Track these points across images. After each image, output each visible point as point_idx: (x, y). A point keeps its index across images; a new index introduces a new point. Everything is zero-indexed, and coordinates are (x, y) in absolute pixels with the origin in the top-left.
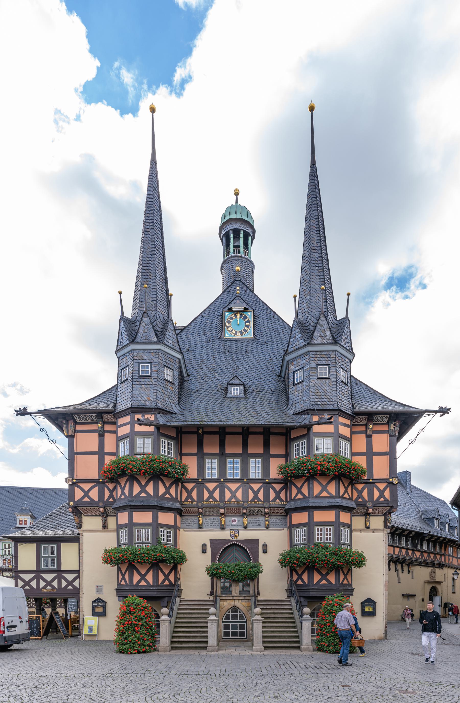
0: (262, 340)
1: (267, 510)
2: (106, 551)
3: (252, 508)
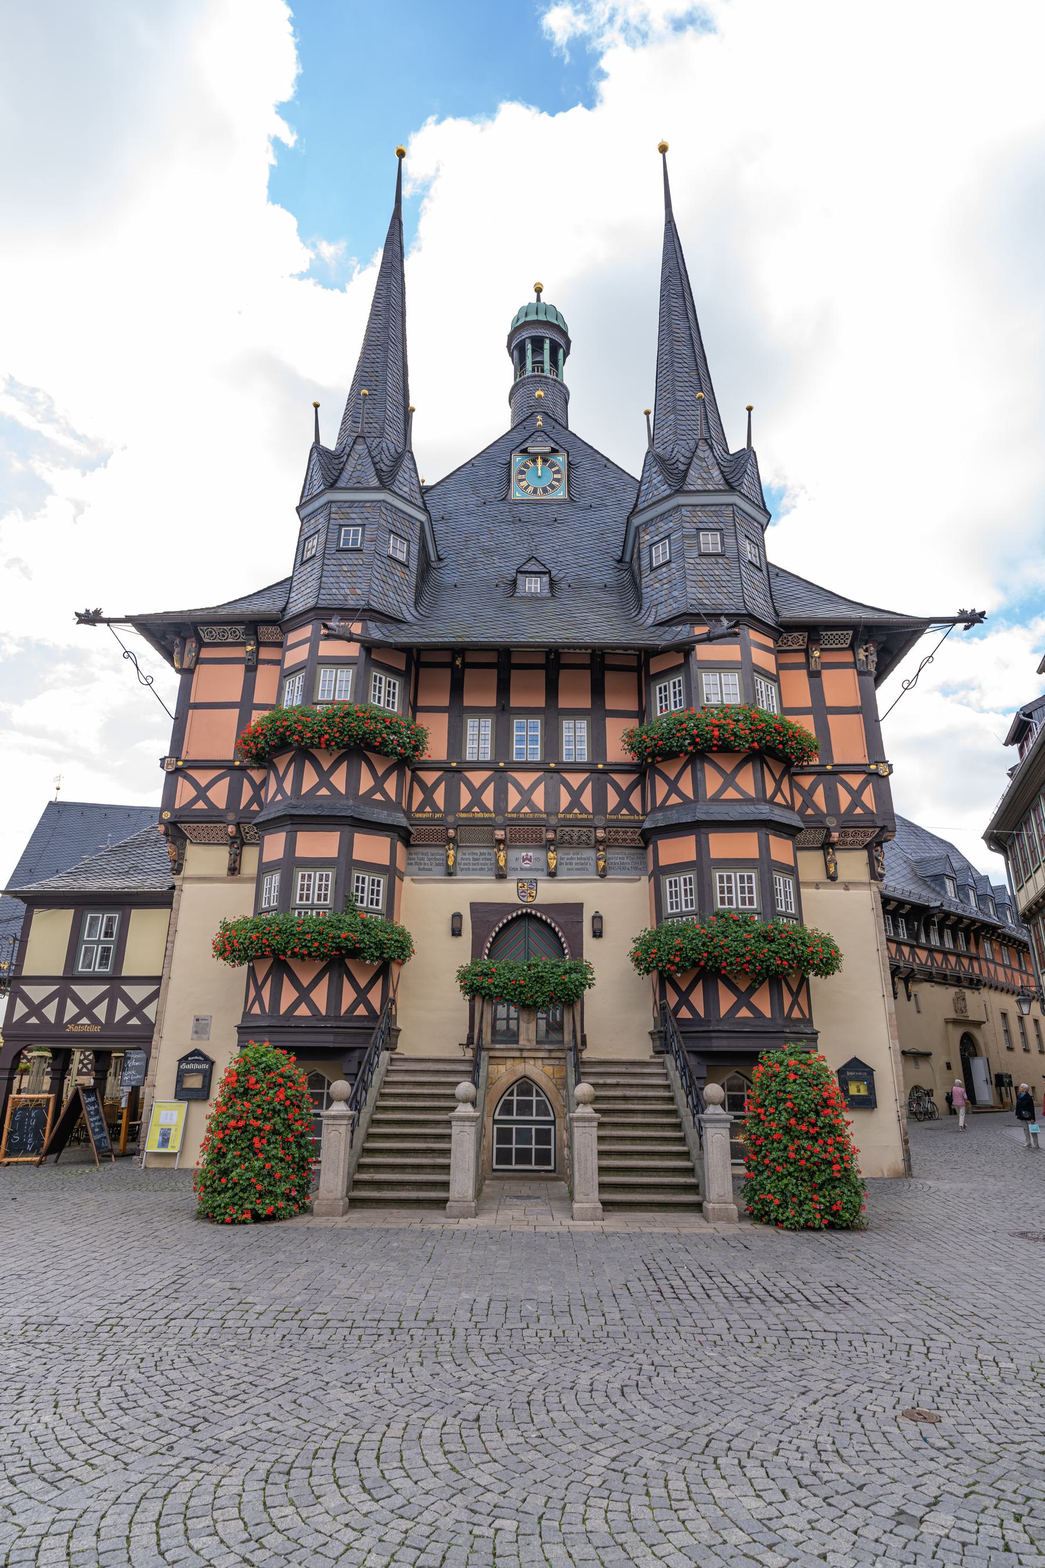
0: (583, 502)
1: (600, 834)
2: (225, 927)
3: (567, 829)
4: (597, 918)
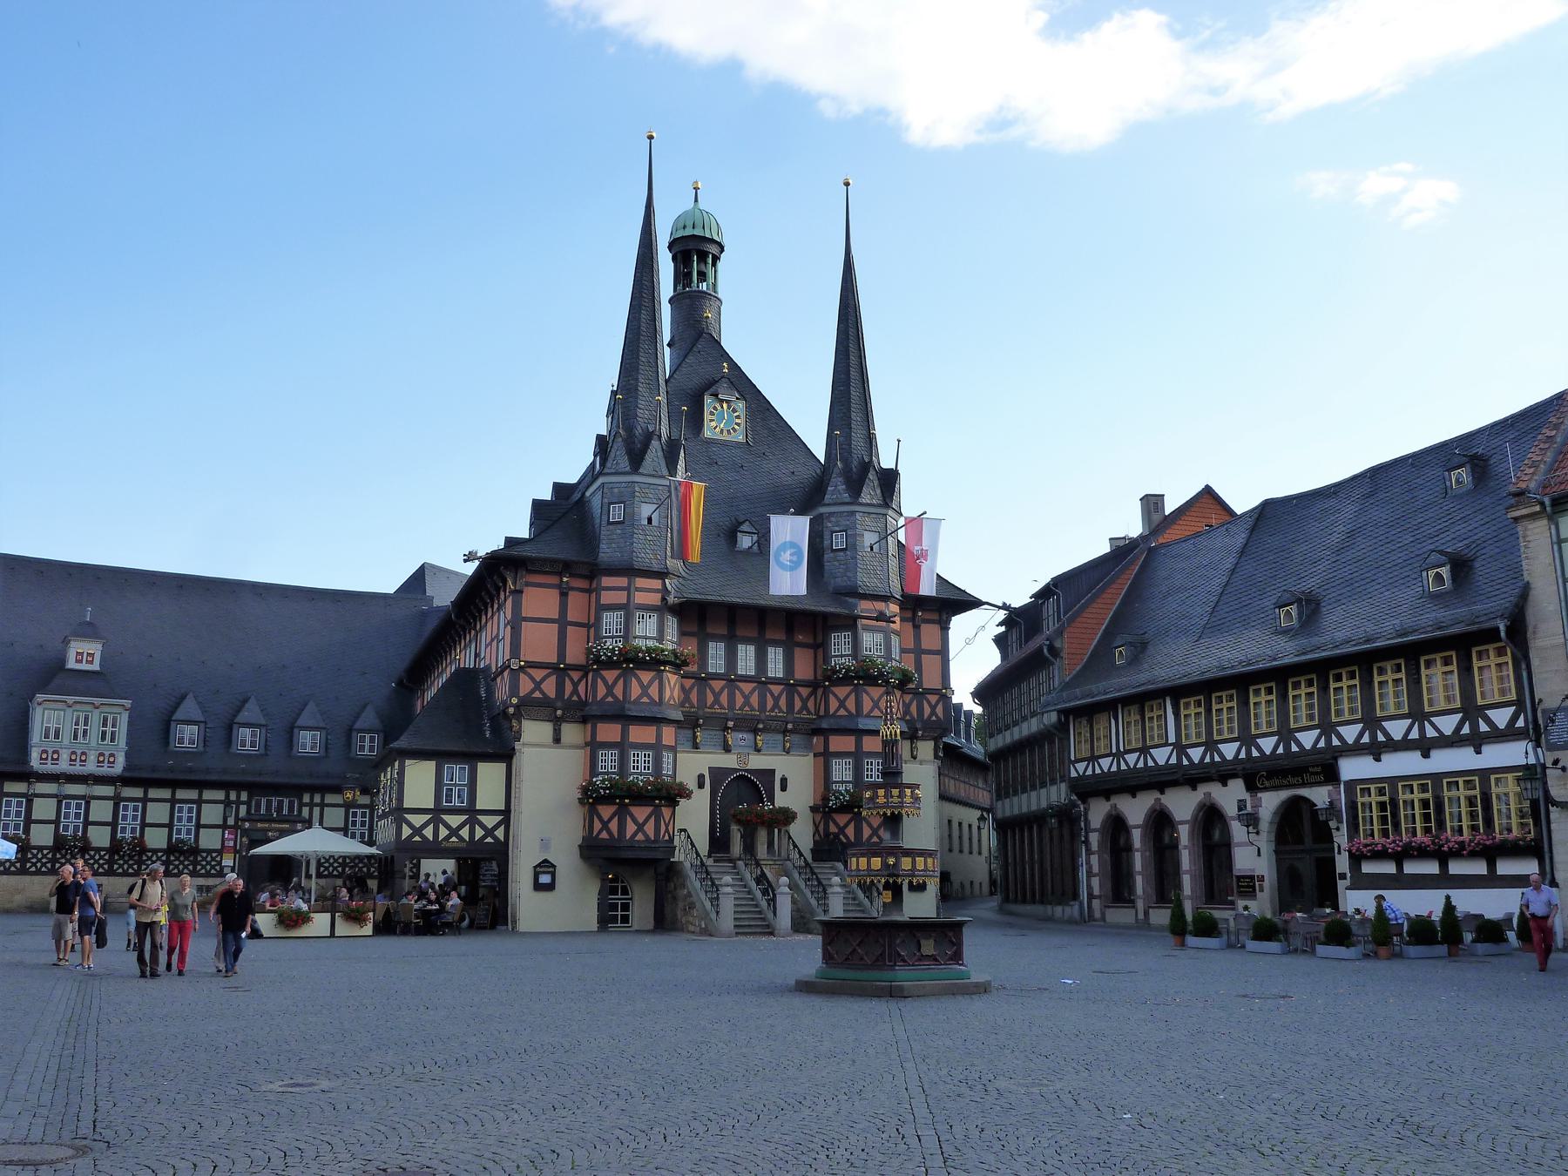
1: (790, 726)
4: (784, 781)
